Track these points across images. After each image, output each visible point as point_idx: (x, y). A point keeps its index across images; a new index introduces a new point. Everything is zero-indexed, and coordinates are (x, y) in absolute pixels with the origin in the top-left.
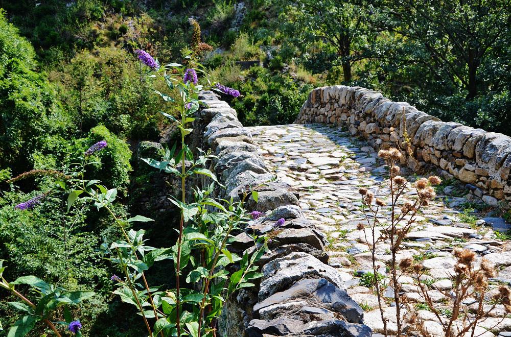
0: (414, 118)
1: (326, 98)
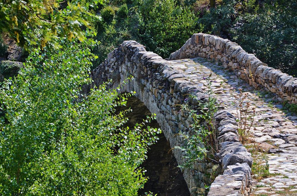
1: (206, 43)
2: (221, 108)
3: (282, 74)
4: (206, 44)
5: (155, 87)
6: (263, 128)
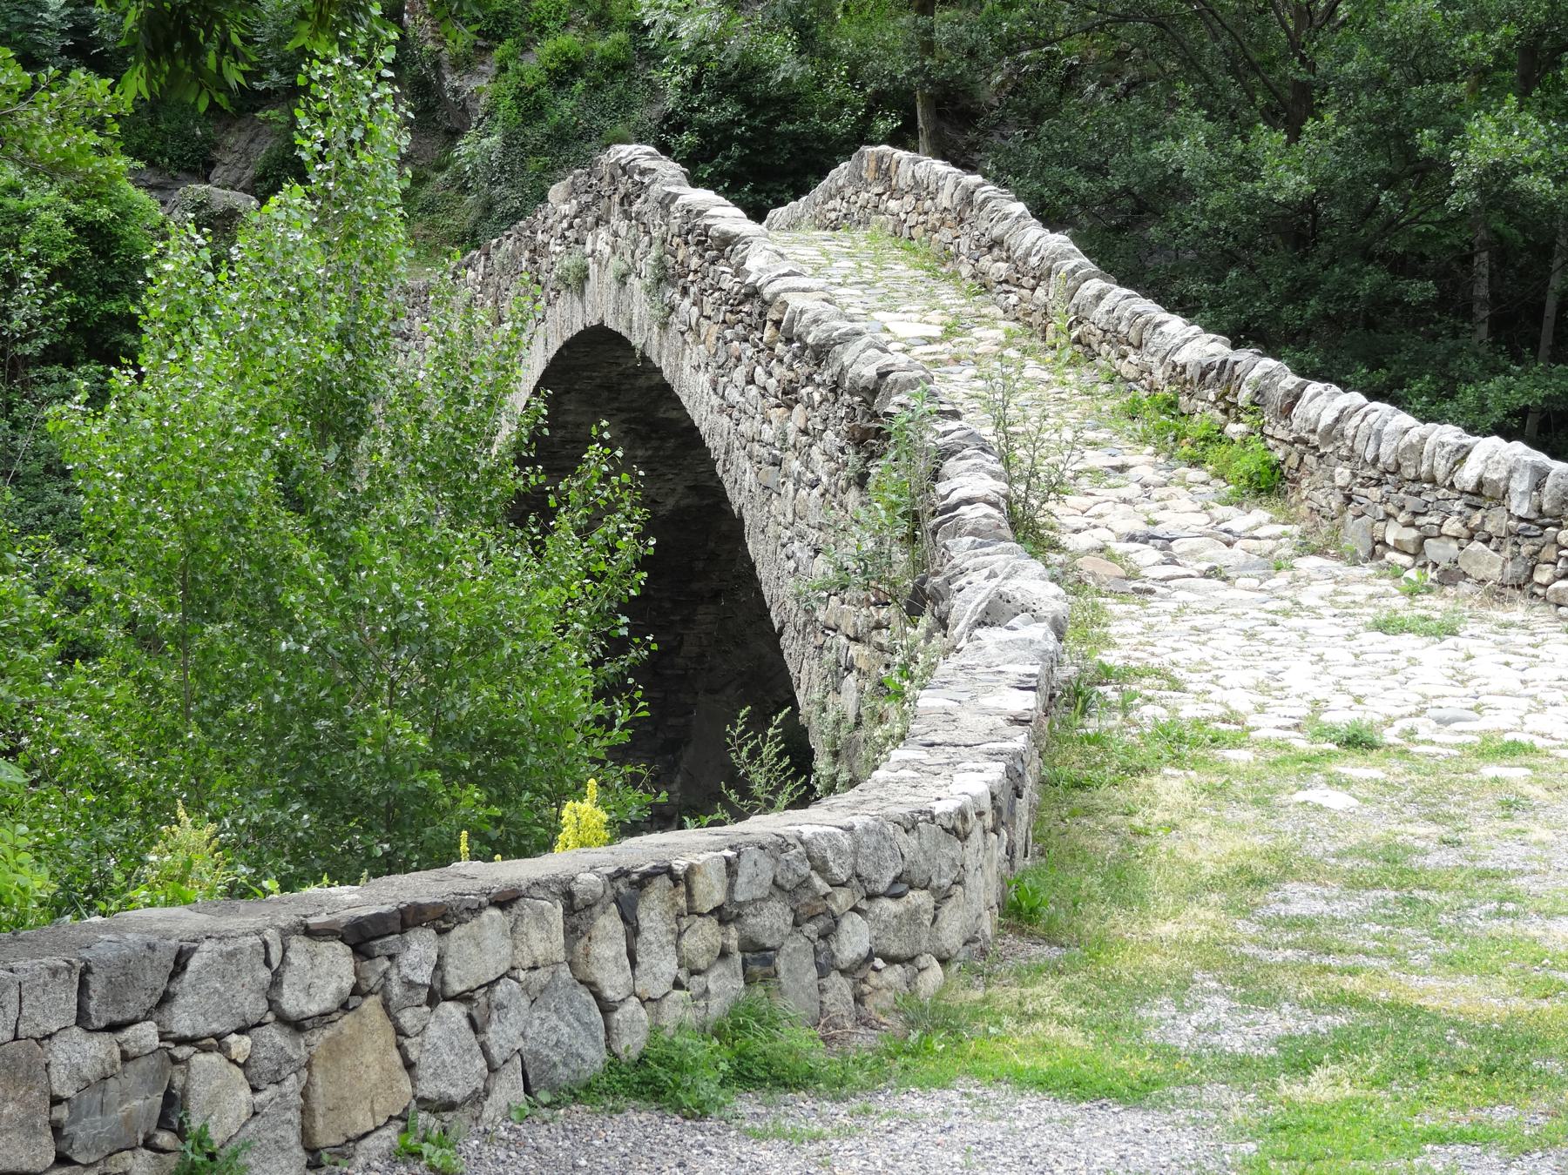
0: (1073, 271)
1: (903, 178)
2: (949, 412)
3: (1166, 316)
4: (902, 184)
5: (709, 318)
6: (1089, 501)
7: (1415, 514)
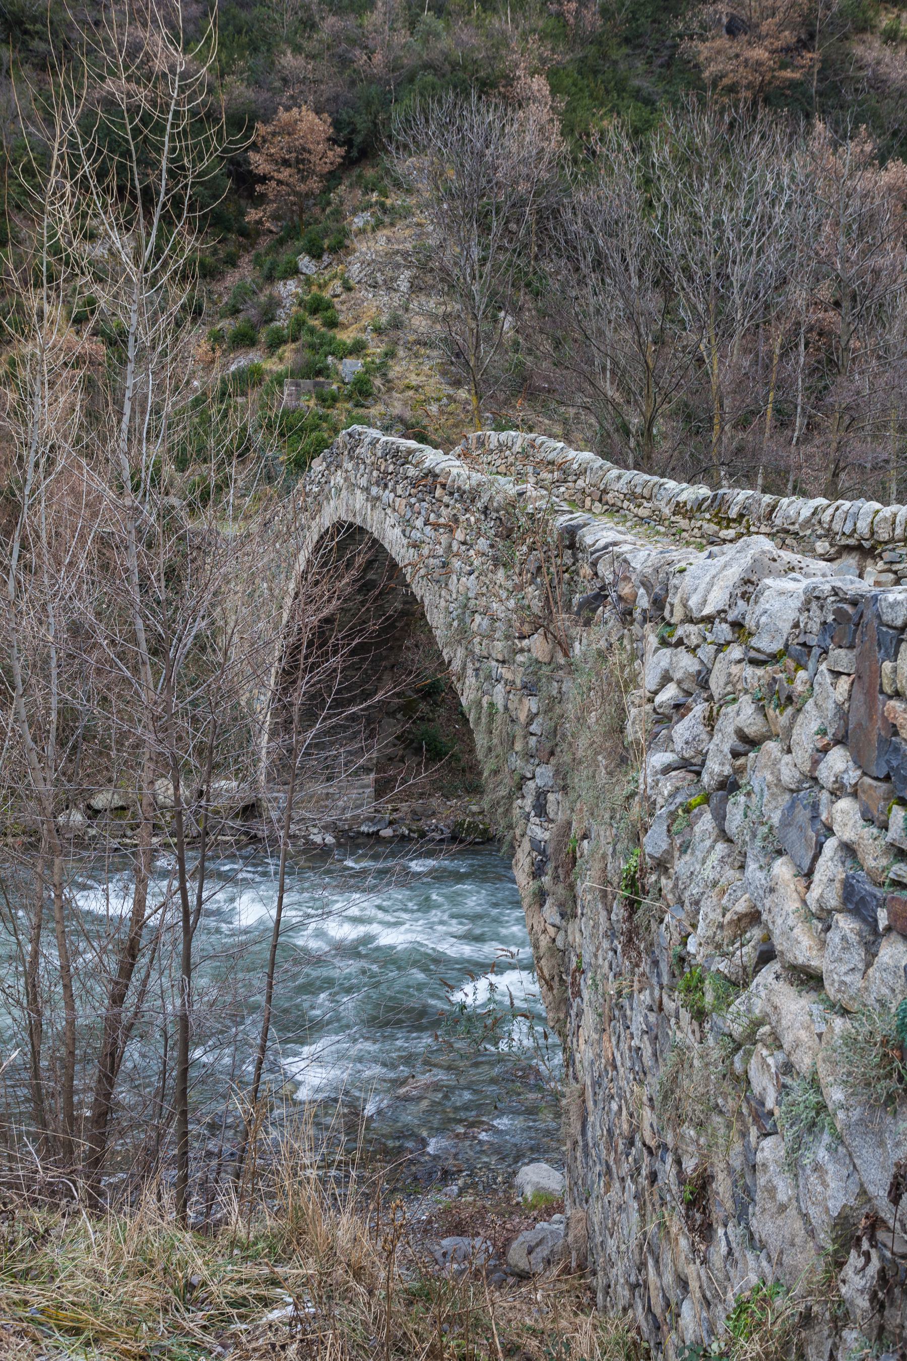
1: (493, 444)
7: (892, 563)
